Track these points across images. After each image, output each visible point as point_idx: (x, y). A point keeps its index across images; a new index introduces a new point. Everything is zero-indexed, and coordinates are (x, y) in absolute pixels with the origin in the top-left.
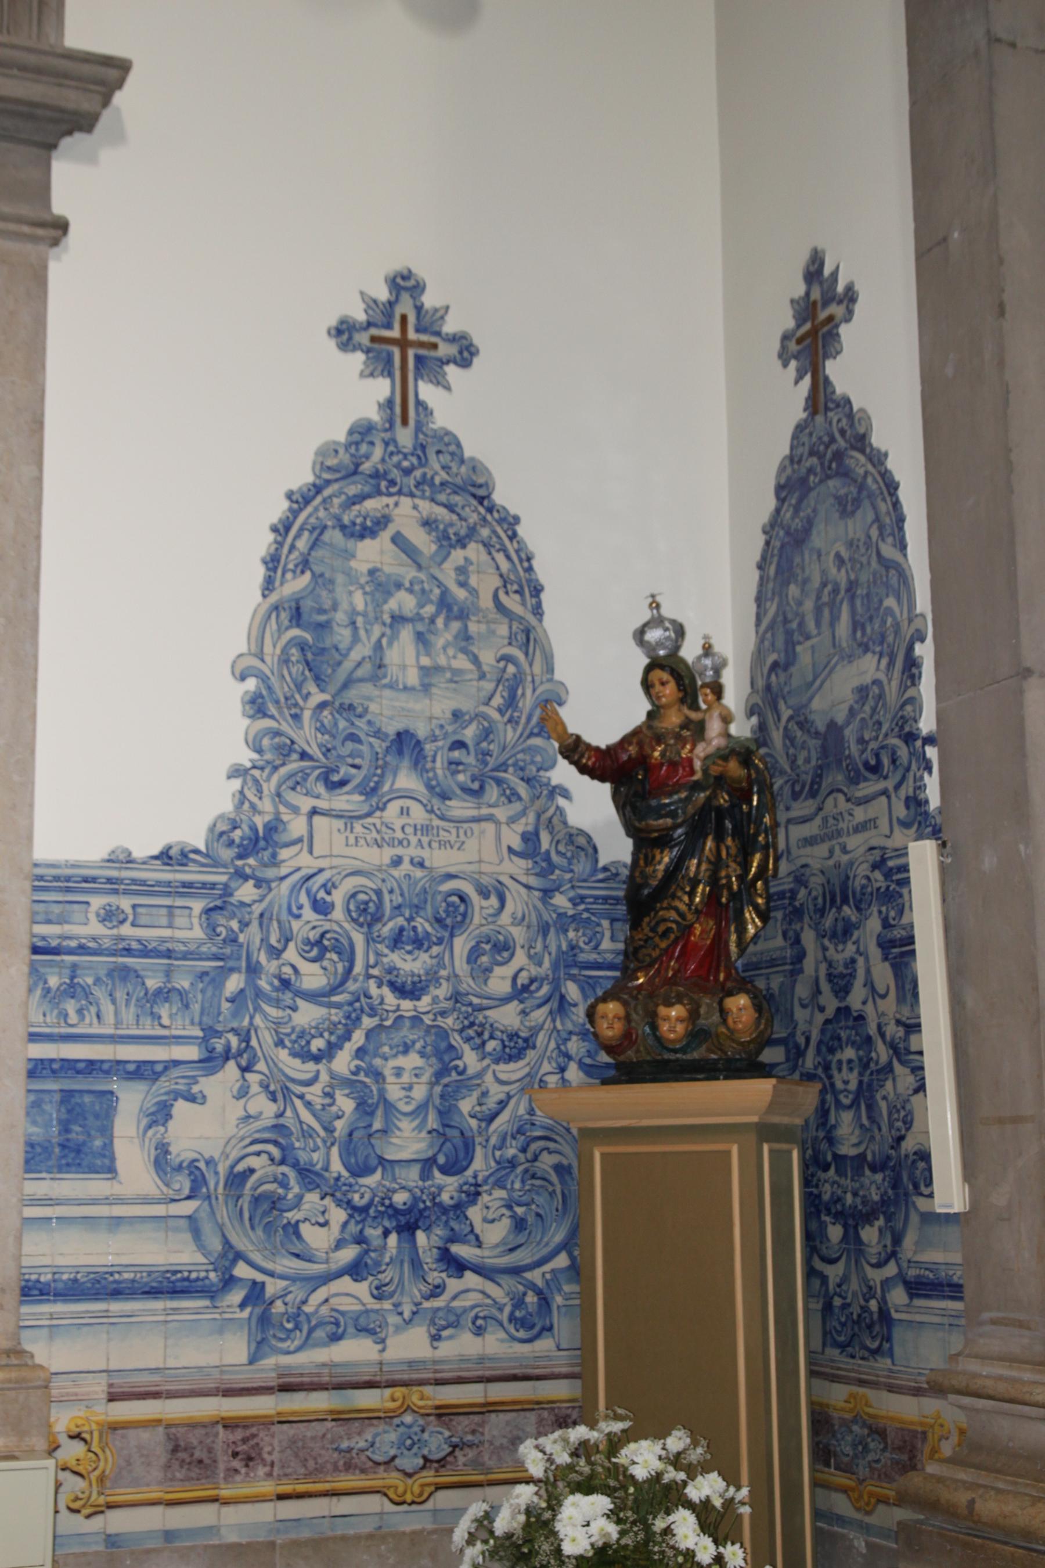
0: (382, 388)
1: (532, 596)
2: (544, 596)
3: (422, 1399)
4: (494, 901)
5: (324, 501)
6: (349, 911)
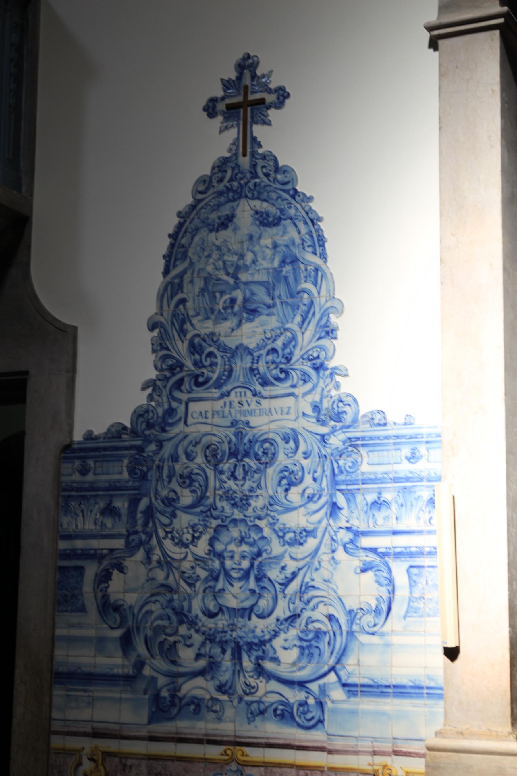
0: (233, 134)
1: (320, 246)
2: (327, 245)
3: (243, 755)
4: (292, 444)
5: (197, 213)
6: (206, 456)
